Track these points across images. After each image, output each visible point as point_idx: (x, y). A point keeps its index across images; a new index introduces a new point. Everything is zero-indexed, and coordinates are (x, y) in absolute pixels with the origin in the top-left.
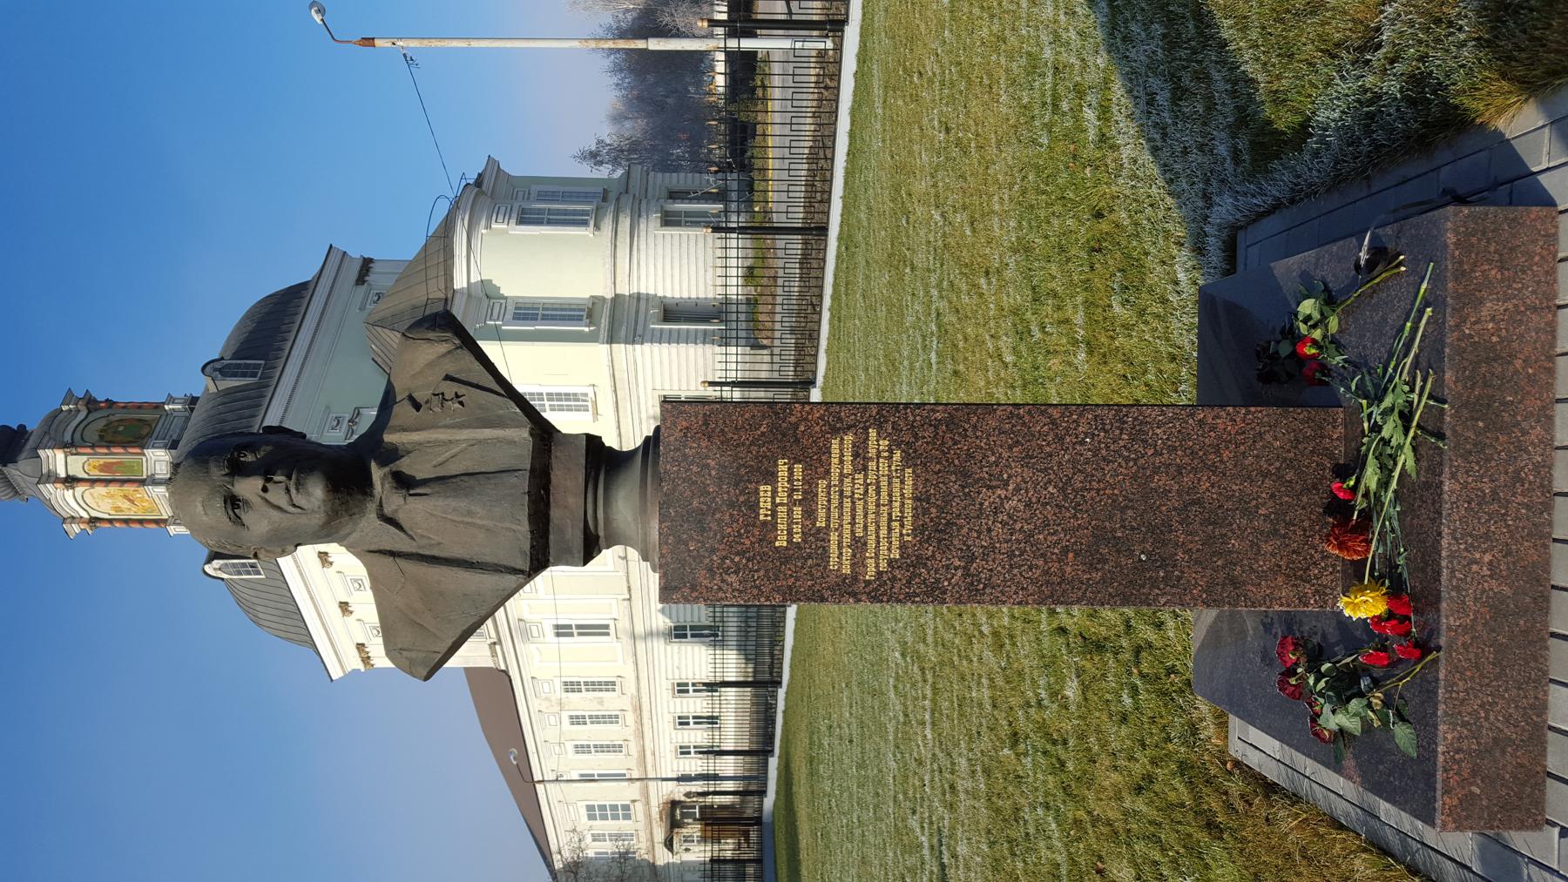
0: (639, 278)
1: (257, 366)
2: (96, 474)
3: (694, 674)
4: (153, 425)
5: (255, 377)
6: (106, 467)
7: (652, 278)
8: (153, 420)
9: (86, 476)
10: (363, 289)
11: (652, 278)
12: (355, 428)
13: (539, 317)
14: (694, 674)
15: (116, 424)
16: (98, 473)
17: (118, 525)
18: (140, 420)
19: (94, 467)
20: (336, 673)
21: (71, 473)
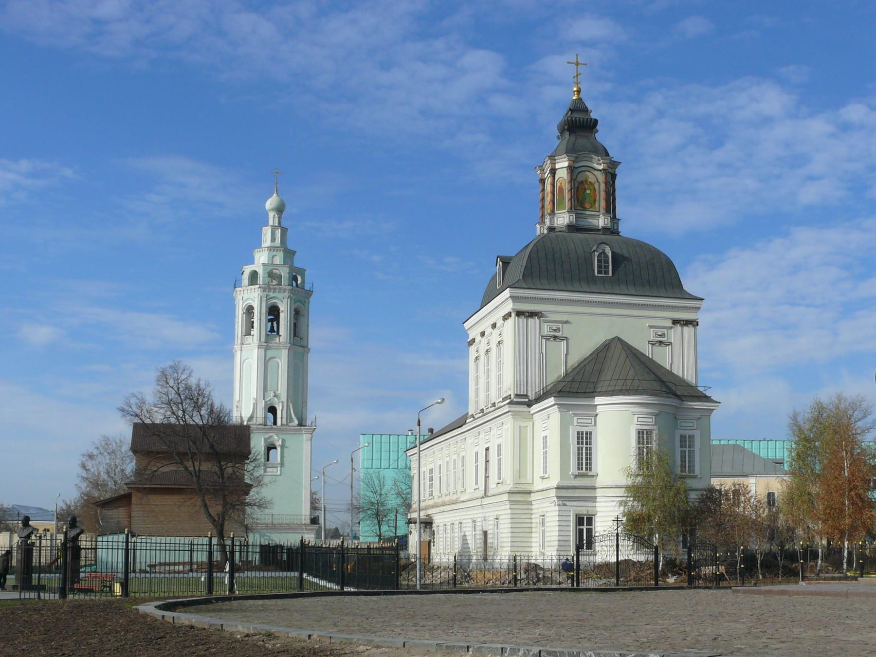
0: (606, 502)
1: (607, 272)
2: (557, 185)
3: (502, 533)
4: (591, 209)
5: (598, 273)
6: (561, 190)
7: (605, 509)
8: (595, 208)
9: (556, 179)
10: (670, 324)
11: (605, 509)
12: (552, 339)
13: (580, 446)
14: (502, 533)
15: (592, 188)
16: (558, 185)
17: (541, 195)
18: (595, 200)
19: (561, 184)
20: (467, 325)
21: (558, 172)
